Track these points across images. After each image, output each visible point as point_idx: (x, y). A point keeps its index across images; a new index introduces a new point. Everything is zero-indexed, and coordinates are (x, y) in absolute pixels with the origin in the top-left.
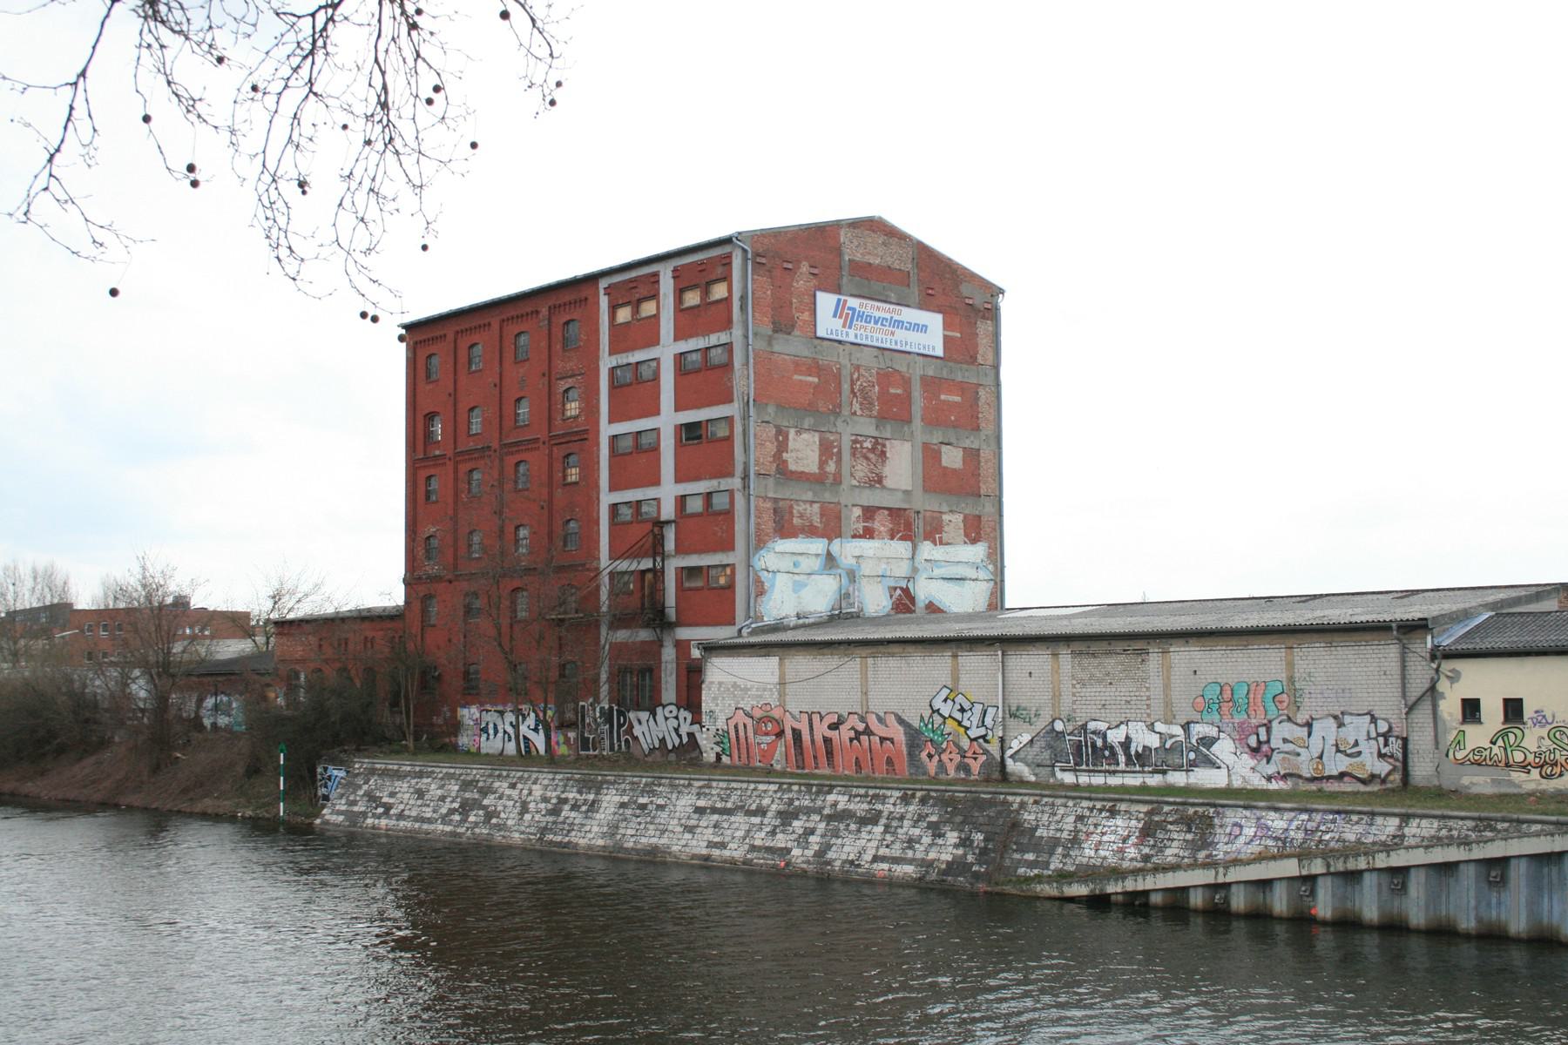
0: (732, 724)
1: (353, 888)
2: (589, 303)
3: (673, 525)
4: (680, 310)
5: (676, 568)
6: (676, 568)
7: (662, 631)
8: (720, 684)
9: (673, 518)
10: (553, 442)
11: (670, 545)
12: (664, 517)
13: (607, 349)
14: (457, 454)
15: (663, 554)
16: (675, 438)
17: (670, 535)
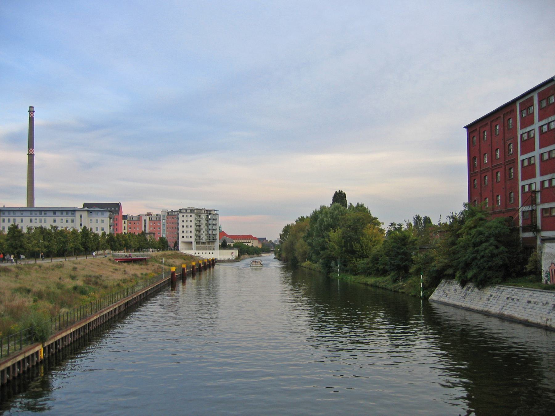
0: (550, 268)
1: (7, 411)
2: (514, 111)
3: (540, 192)
4: (540, 109)
5: (541, 209)
6: (541, 209)
7: (537, 233)
8: (547, 253)
9: (539, 190)
10: (506, 164)
11: (538, 200)
12: (537, 190)
13: (519, 127)
14: (493, 167)
15: (536, 204)
16: (540, 159)
17: (539, 196)
